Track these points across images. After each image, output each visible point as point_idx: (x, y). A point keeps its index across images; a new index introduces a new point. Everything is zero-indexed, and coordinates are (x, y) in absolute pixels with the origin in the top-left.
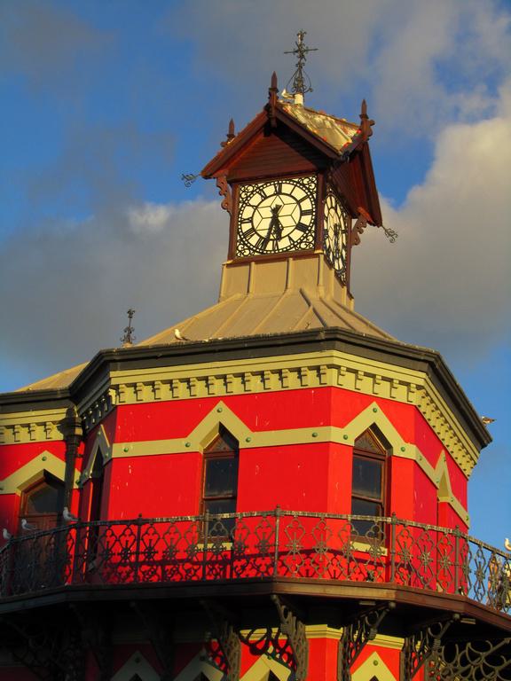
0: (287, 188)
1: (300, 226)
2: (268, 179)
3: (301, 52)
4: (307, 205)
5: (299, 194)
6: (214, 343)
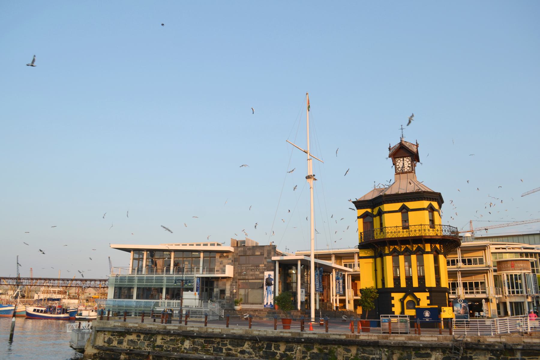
0: (405, 159)
1: (408, 167)
2: (401, 157)
3: (402, 129)
4: (410, 162)
5: (408, 160)
6: (402, 194)
